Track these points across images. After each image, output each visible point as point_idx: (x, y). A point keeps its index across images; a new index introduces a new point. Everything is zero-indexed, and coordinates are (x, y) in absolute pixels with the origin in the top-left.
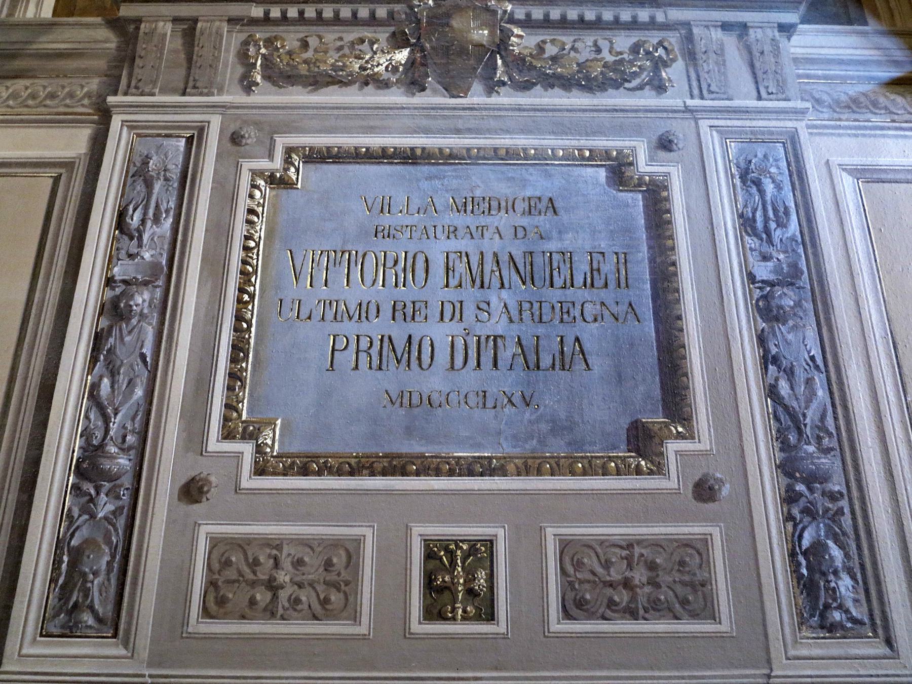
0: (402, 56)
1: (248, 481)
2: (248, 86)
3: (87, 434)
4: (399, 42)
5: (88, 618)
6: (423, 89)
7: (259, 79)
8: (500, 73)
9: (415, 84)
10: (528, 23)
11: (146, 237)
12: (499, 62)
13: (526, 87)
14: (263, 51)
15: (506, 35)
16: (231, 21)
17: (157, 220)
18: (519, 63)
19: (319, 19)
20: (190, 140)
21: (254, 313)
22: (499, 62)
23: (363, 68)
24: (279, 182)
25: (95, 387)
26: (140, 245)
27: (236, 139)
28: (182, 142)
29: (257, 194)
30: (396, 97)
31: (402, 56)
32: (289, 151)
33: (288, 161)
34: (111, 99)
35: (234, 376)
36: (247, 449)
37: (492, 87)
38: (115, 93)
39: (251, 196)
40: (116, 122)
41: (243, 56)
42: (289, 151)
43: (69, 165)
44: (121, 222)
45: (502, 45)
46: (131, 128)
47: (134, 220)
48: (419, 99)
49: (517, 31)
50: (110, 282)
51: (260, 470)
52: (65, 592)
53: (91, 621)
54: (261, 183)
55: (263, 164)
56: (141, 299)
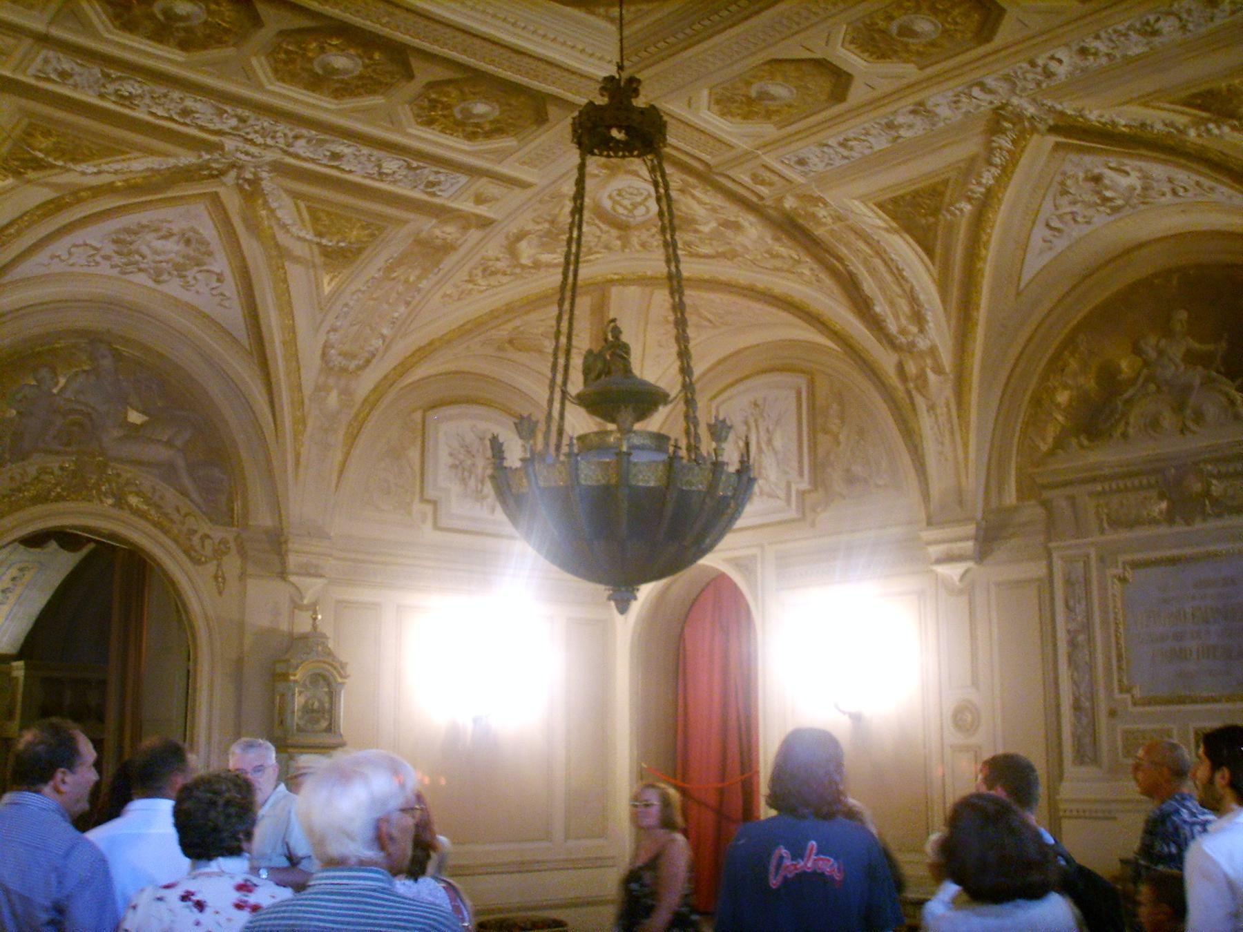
0: (1164, 505)
1: (1130, 708)
2: (1102, 532)
3: (1074, 694)
4: (1162, 496)
5: (1087, 760)
6: (1175, 522)
7: (1105, 525)
8: (1208, 509)
9: (1171, 521)
10: (1219, 476)
11: (1077, 611)
12: (1207, 502)
13: (1219, 516)
14: (1106, 511)
15: (1209, 485)
16: (1090, 494)
17: (1079, 603)
18: (1215, 502)
19: (1127, 489)
20: (1085, 562)
21: (1122, 642)
22: (1207, 502)
23: (1148, 515)
24: (1123, 580)
25: (1072, 675)
26: (1075, 615)
27: (1102, 560)
28: (1082, 564)
29: (1115, 586)
30: (1164, 530)
31: (1164, 505)
32: (1124, 563)
33: (1124, 568)
34: (1051, 545)
35: (1120, 668)
36: (1128, 696)
37: (1204, 520)
38: (1050, 541)
39: (1113, 588)
40: (1055, 555)
41: (1097, 513)
42: (1124, 563)
43: (1039, 580)
44: (1067, 606)
45: (1207, 493)
46: (1062, 558)
47: (1071, 603)
48: (1175, 529)
49: (1214, 482)
50: (1069, 632)
51: (1135, 704)
52: (1078, 751)
53: (1088, 760)
54: (1115, 580)
55: (1114, 571)
56: (1081, 638)
